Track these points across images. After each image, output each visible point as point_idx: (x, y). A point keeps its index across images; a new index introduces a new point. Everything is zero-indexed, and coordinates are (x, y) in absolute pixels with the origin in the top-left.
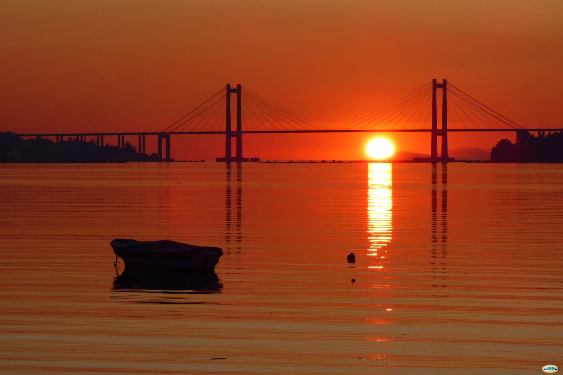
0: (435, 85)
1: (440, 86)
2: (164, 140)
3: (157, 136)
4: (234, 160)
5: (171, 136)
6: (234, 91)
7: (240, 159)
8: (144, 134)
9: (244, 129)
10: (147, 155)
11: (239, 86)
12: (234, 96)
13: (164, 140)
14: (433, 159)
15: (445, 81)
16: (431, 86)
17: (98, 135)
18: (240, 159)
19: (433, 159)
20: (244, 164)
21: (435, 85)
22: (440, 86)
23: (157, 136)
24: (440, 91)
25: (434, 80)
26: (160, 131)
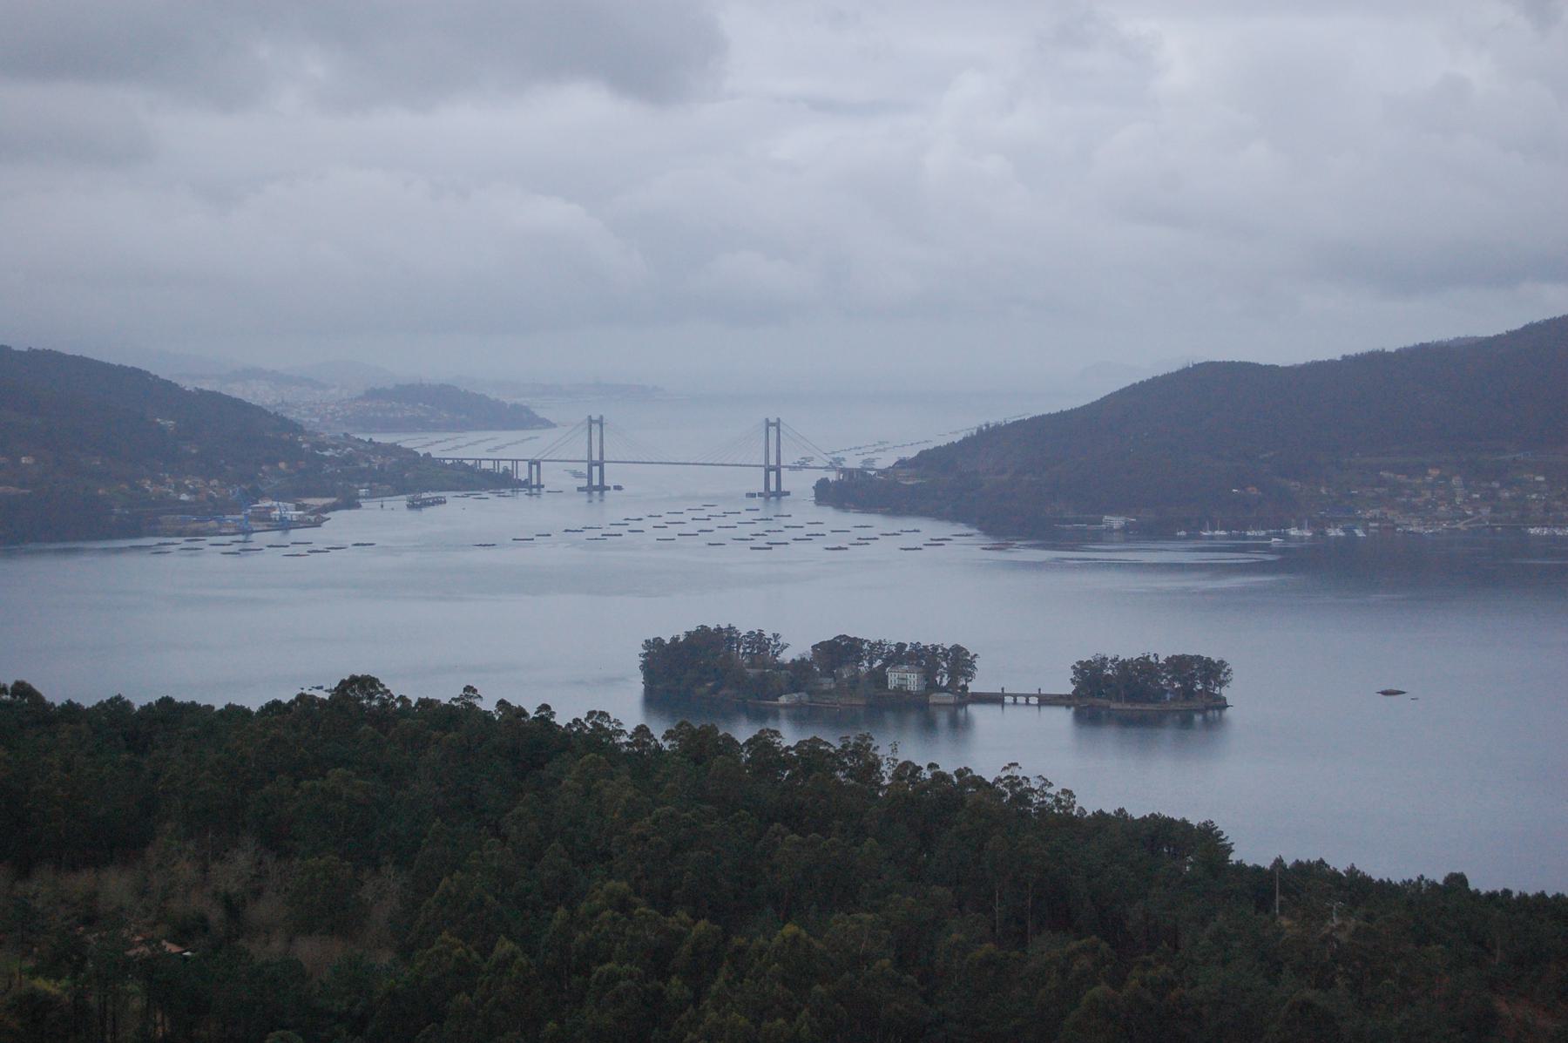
0: (768, 424)
1: (773, 424)
2: (534, 467)
3: (527, 463)
4: (596, 488)
5: (542, 463)
6: (596, 422)
7: (602, 488)
8: (517, 461)
9: (605, 458)
10: (520, 480)
11: (601, 417)
12: (596, 428)
13: (534, 467)
14: (767, 495)
15: (779, 419)
16: (764, 425)
17: (476, 460)
18: (602, 488)
19: (767, 495)
20: (606, 492)
21: (768, 424)
22: (773, 424)
23: (527, 463)
24: (773, 430)
25: (767, 420)
26: (530, 457)
